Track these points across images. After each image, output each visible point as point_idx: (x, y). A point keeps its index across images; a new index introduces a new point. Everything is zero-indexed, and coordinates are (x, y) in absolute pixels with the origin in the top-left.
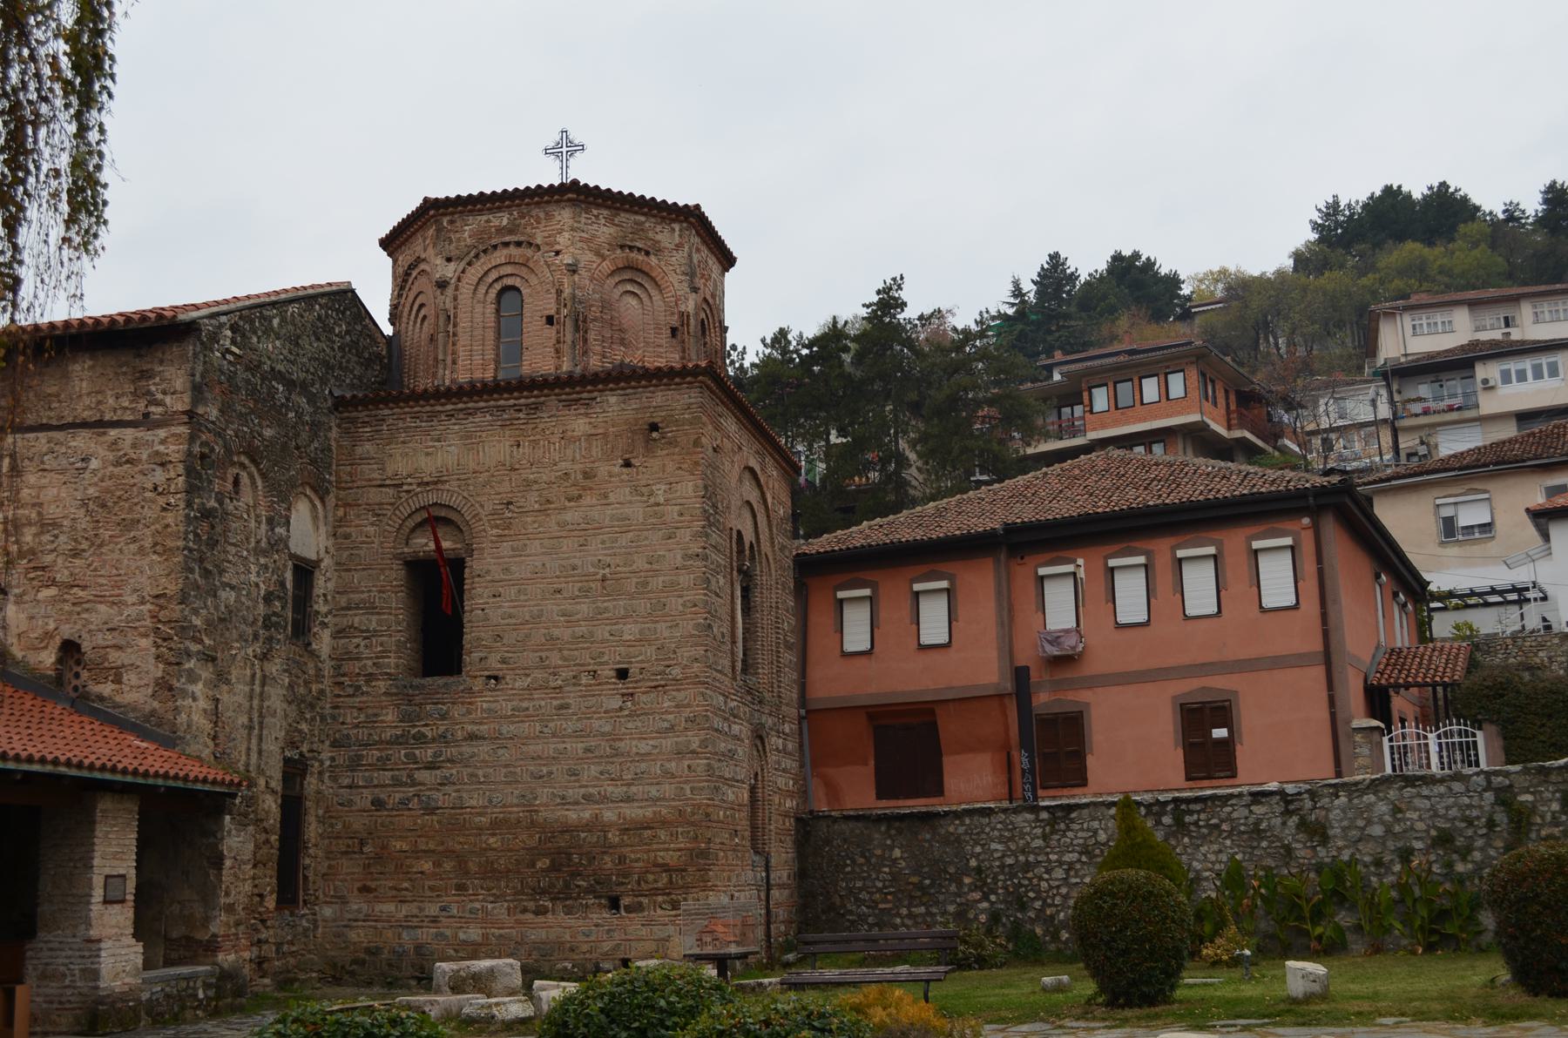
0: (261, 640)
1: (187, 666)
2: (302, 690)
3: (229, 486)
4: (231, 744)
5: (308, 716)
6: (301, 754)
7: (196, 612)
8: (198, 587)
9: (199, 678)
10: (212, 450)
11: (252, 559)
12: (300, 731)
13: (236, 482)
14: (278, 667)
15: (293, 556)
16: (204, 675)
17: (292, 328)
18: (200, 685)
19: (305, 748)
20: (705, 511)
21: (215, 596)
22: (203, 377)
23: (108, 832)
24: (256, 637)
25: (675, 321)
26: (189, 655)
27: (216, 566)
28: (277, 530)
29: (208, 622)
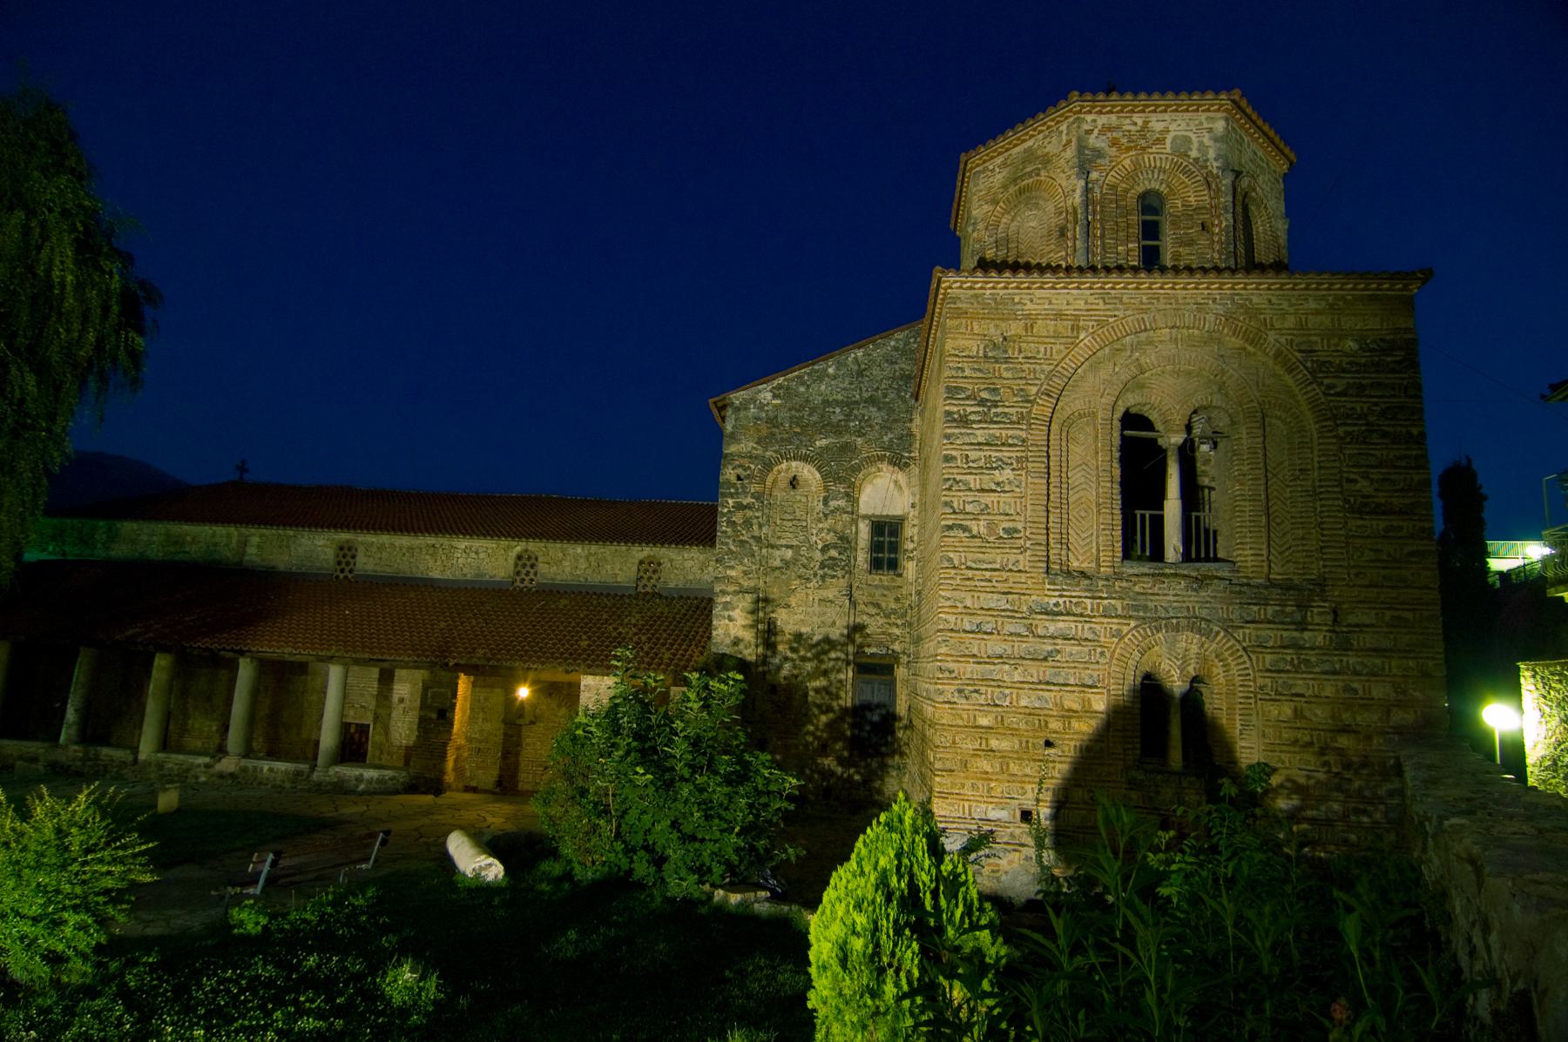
0: (818, 577)
1: (724, 600)
2: (893, 606)
3: (783, 482)
5: (899, 622)
7: (732, 568)
8: (732, 552)
10: (749, 468)
12: (890, 634)
13: (794, 483)
15: (865, 517)
17: (855, 368)
18: (738, 611)
19: (897, 647)
20: (948, 413)
21: (753, 556)
24: (815, 575)
25: (1060, 220)
26: (724, 593)
27: (753, 537)
28: (833, 504)
29: (745, 573)
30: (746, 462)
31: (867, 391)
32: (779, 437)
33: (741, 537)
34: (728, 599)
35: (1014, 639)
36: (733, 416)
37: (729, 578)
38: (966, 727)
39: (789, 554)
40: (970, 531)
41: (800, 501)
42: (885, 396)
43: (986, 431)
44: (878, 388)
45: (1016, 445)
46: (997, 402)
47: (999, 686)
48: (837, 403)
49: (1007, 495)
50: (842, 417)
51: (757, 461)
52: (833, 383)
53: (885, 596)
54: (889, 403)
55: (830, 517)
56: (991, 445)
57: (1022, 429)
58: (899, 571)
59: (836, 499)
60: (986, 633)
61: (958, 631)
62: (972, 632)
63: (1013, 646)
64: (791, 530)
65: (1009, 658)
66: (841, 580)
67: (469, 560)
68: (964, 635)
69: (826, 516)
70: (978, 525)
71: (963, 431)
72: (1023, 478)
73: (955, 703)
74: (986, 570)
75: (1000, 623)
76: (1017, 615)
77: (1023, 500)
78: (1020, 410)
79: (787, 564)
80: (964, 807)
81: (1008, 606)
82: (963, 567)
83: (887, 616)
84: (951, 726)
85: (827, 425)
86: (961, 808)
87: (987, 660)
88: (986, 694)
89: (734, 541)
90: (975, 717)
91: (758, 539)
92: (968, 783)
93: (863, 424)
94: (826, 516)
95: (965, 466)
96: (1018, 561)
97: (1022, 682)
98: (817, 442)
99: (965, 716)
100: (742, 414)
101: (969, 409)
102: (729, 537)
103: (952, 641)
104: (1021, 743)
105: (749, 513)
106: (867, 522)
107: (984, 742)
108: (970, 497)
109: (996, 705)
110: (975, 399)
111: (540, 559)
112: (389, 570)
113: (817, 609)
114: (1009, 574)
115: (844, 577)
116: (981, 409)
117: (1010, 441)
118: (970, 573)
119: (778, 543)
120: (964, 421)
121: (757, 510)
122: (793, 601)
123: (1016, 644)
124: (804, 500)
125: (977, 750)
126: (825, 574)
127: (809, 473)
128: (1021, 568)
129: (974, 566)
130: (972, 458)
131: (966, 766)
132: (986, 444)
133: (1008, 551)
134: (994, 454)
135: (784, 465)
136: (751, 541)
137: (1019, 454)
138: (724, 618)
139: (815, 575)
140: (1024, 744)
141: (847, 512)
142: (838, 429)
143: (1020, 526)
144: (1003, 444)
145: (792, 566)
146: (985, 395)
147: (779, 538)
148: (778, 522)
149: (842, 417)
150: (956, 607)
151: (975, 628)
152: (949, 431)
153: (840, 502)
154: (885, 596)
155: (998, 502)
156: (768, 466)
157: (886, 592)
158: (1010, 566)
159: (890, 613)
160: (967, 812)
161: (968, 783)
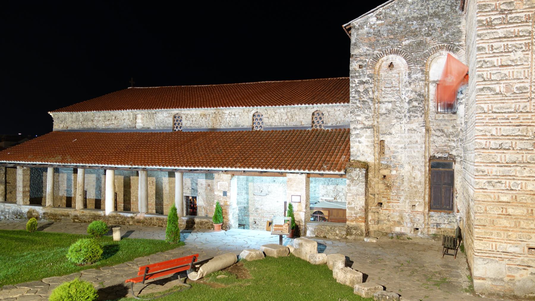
0: (407, 117)
1: (356, 132)
2: (451, 130)
4: (394, 154)
5: (455, 140)
6: (449, 154)
7: (359, 115)
9: (363, 136)
10: (366, 61)
11: (403, 89)
13: (391, 65)
14: (417, 125)
15: (434, 82)
16: (365, 136)
19: (454, 153)
20: (480, 21)
21: (370, 108)
22: (356, 39)
23: (292, 184)
24: (405, 116)
29: (366, 118)
30: (363, 58)
31: (432, 9)
32: (381, 42)
33: (363, 99)
34: (358, 132)
35: (524, 152)
36: (355, 34)
37: (358, 121)
38: (493, 202)
39: (390, 106)
40: (495, 90)
41: (395, 77)
42: (443, 10)
43: (505, 30)
44: (439, 6)
45: (525, 36)
46: (511, 10)
47: (514, 179)
48: (415, 19)
49: (519, 67)
50: (417, 26)
51: (369, 57)
52: (411, 7)
53: (446, 125)
54: (446, 14)
55: (412, 84)
56: (508, 38)
57: (529, 26)
58: (454, 110)
59: (415, 73)
60: (505, 149)
61: (488, 149)
62: (497, 149)
63: (523, 156)
64: (390, 93)
65: (520, 163)
66: (420, 118)
67: (231, 119)
68: (491, 151)
69: (410, 83)
70: (500, 87)
71: (489, 31)
72: (530, 56)
73: (486, 189)
74: (505, 113)
75: (514, 143)
76: (525, 138)
77: (529, 69)
78: (527, 13)
79: (389, 112)
80: (492, 245)
81: (519, 133)
82: (490, 112)
83: (448, 136)
84: (484, 201)
85: (409, 32)
86: (491, 246)
87: (507, 165)
88: (505, 183)
89: (359, 101)
90: (499, 197)
91: (372, 99)
92: (495, 232)
93: (430, 29)
94: (410, 83)
95: (491, 52)
96: (526, 106)
97: (529, 177)
98: (403, 43)
99: (492, 196)
100: (361, 31)
101: (493, 17)
102: (356, 100)
103: (484, 154)
104: (528, 211)
105: (367, 86)
106: (434, 84)
107: (504, 210)
108: (494, 70)
109: (512, 190)
110: (497, 10)
111: (264, 116)
112: (197, 126)
113: (407, 134)
114: (520, 114)
115: (421, 116)
116: (501, 16)
117: (521, 34)
118: (495, 115)
119: (384, 100)
120: (490, 25)
121: (371, 83)
122: (393, 131)
123: (525, 155)
124: (397, 75)
125: (500, 214)
126: (411, 115)
127: (399, 61)
128: (528, 110)
129: (497, 111)
130: (495, 47)
131: (493, 223)
132: (505, 37)
133: (519, 100)
134: (509, 43)
135: (385, 57)
136: (369, 101)
137: (527, 42)
138: (356, 142)
139: (405, 116)
140: (530, 211)
141: (423, 80)
142: (415, 34)
143: (527, 85)
144: (516, 36)
145: (392, 112)
146: (503, 7)
147: (384, 97)
148: (383, 89)
149: (417, 26)
150: (486, 135)
151: (498, 146)
152: (480, 32)
153: (418, 75)
154: (446, 125)
155: (513, 72)
156: (376, 59)
157: (447, 123)
158: (521, 110)
159: (450, 135)
160: (494, 247)
161: (495, 232)
